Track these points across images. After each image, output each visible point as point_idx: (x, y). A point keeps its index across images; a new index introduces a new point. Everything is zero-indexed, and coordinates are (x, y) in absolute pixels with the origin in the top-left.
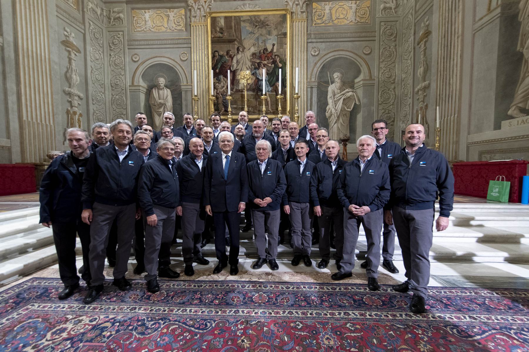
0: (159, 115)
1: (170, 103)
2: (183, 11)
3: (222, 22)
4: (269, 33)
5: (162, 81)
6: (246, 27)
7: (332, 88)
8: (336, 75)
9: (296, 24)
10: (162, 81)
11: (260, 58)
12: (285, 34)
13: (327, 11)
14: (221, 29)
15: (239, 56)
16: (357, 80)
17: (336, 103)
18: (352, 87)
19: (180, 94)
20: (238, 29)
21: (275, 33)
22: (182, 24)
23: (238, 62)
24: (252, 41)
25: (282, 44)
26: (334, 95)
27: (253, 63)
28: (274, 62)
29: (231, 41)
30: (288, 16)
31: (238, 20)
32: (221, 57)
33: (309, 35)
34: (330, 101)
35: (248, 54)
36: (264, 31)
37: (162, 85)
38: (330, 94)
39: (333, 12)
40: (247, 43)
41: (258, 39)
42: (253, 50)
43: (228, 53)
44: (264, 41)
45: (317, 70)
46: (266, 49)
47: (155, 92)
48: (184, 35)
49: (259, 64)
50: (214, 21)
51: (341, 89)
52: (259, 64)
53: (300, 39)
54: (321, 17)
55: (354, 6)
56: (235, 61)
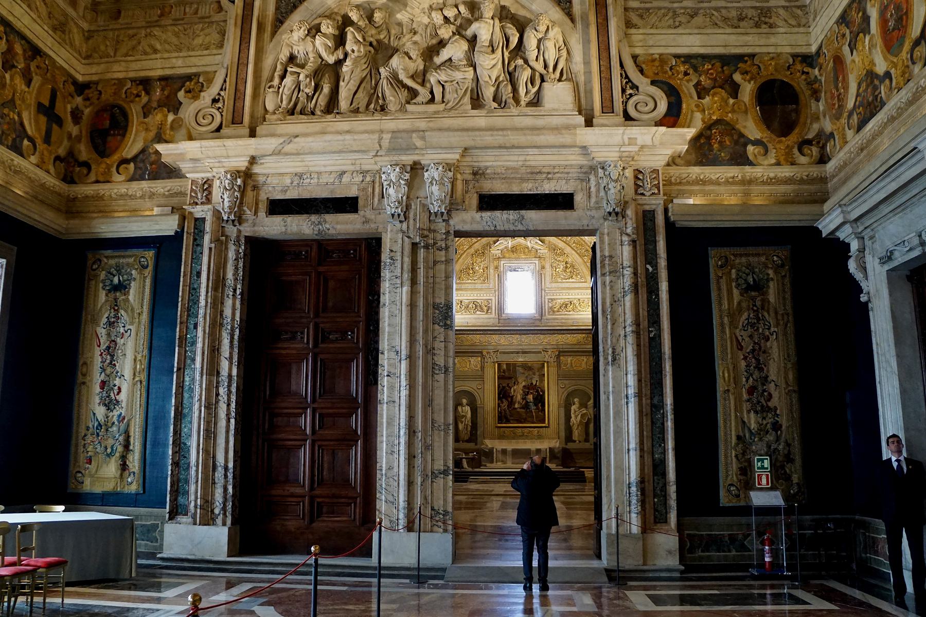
0: (462, 423)
1: (469, 415)
2: (479, 359)
3: (505, 367)
4: (534, 374)
5: (464, 401)
6: (520, 370)
7: (573, 408)
8: (576, 400)
9: (551, 369)
10: (464, 401)
11: (528, 388)
12: (544, 375)
13: (569, 362)
14: (504, 370)
15: (515, 387)
16: (589, 403)
17: (576, 417)
18: (586, 407)
19: (476, 410)
20: (515, 371)
21: (537, 373)
22: (479, 366)
23: (514, 391)
24: (524, 378)
25: (542, 380)
26: (575, 412)
27: (524, 392)
28: (537, 391)
29: (510, 378)
30: (546, 365)
31: (515, 365)
32: (504, 387)
33: (558, 375)
34: (573, 416)
35: (521, 386)
36: (531, 373)
37: (465, 404)
38: (572, 411)
39: (573, 362)
40: (520, 381)
41: (527, 377)
42: (524, 384)
43: (508, 384)
44: (531, 379)
45: (564, 397)
46: (532, 384)
47: (459, 408)
48: (480, 373)
49: (528, 392)
50: (499, 365)
51: (579, 408)
52: (528, 392)
53: (554, 377)
54: (566, 365)
55: (585, 360)
56: (512, 390)
